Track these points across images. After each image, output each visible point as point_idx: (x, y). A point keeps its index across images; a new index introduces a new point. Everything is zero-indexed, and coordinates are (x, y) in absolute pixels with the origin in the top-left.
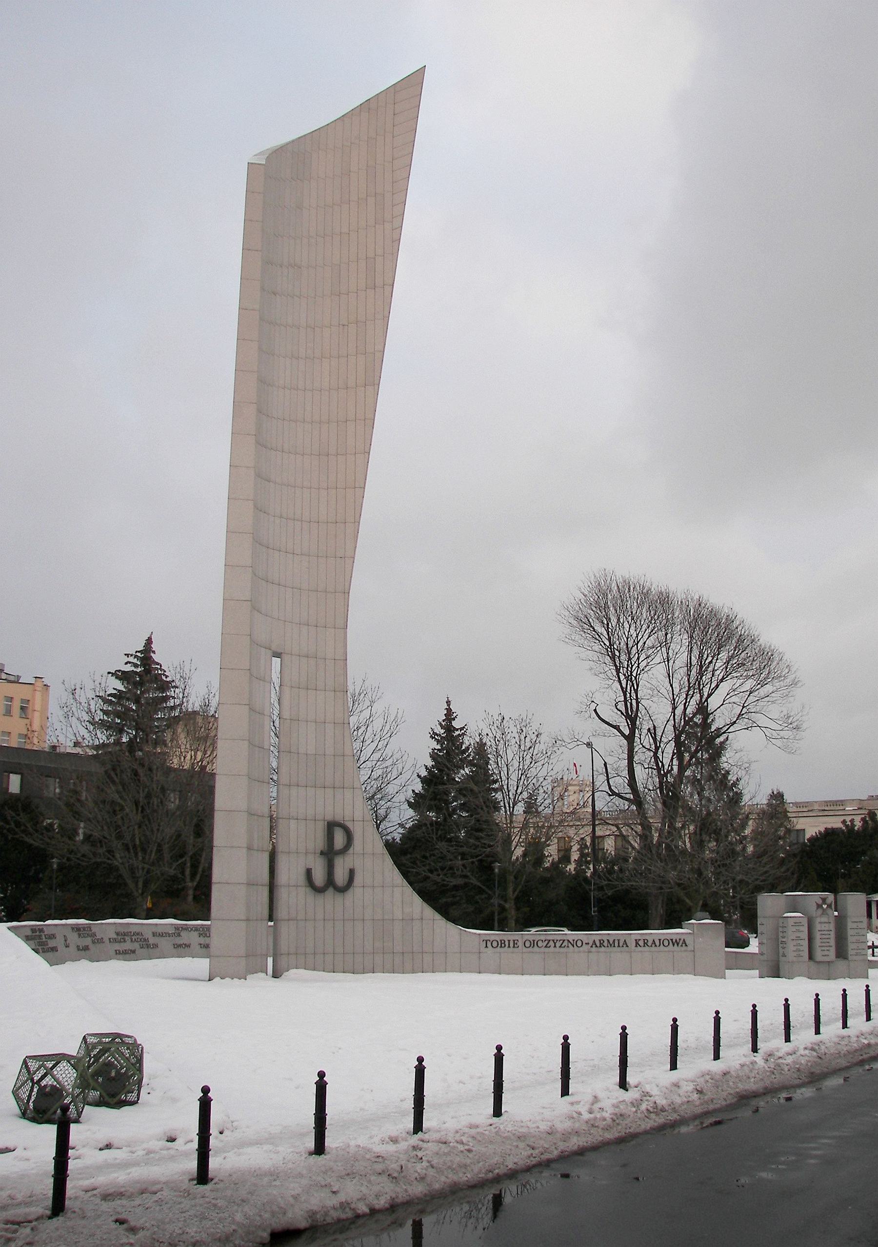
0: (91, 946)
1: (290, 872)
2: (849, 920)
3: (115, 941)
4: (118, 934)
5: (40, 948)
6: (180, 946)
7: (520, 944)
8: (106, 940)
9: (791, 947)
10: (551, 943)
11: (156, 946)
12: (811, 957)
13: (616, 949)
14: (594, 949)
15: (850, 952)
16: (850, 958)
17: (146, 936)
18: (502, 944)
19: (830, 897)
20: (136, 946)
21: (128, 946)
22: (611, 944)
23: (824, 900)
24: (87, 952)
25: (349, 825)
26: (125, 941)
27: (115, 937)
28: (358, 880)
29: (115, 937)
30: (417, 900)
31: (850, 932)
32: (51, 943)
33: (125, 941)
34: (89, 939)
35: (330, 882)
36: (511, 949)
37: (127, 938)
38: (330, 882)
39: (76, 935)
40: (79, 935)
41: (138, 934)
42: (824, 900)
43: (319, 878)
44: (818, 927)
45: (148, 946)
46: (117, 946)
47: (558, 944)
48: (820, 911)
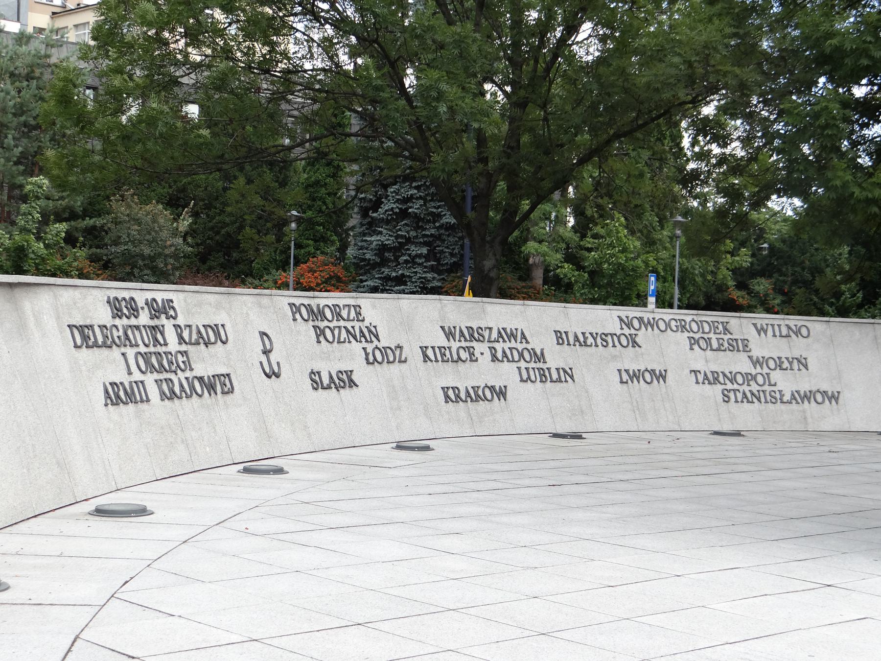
0: (362, 372)
3: (443, 355)
4: (449, 334)
5: (150, 380)
6: (635, 376)
11: (567, 374)
17: (536, 344)
20: (506, 374)
21: (483, 372)
24: (345, 393)
26: (473, 359)
27: (442, 341)
29: (442, 341)
32: (206, 362)
33: (473, 359)
34: (356, 347)
39: (306, 330)
40: (320, 333)
41: (512, 336)
45: (544, 376)
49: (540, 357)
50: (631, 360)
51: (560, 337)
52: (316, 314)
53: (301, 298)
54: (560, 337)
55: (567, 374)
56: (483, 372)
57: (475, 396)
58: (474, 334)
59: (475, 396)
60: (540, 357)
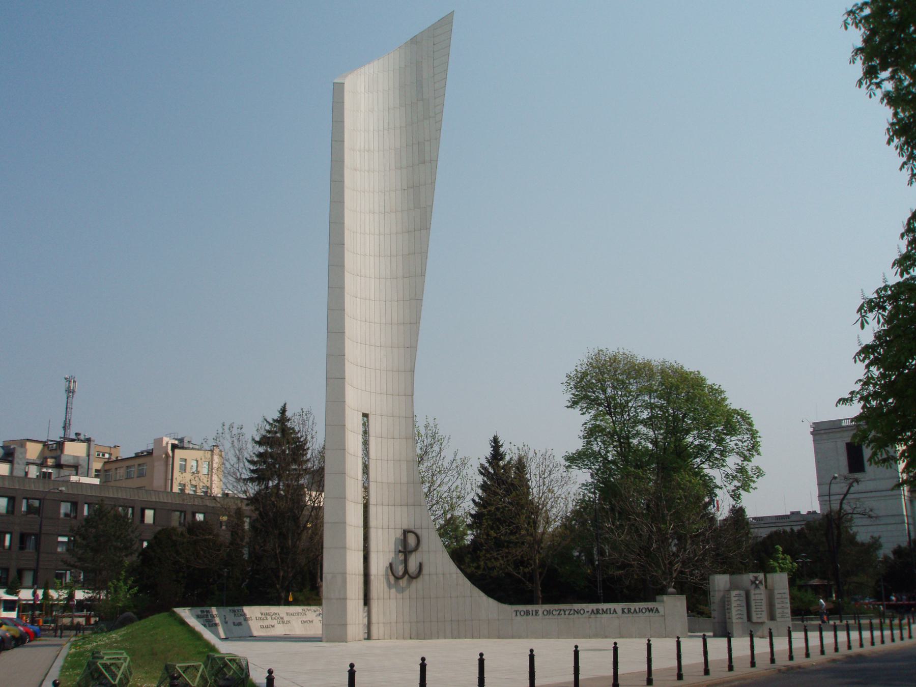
1: (378, 566)
2: (776, 592)
6: (305, 622)
7: (540, 613)
8: (254, 618)
9: (734, 612)
10: (562, 612)
11: (289, 622)
12: (749, 618)
13: (608, 616)
14: (593, 616)
15: (778, 615)
16: (778, 620)
18: (527, 613)
19: (761, 576)
20: (275, 622)
21: (269, 622)
22: (605, 612)
23: (756, 578)
25: (418, 532)
28: (425, 570)
30: (468, 583)
31: (777, 601)
35: (406, 572)
36: (534, 617)
37: (269, 617)
38: (406, 572)
42: (756, 578)
43: (400, 570)
44: (753, 597)
46: (262, 623)
47: (567, 613)
48: (754, 586)
49: (282, 618)
50: (305, 618)
51: (287, 614)
52: (234, 611)
53: (231, 608)
54: (287, 614)
55: (289, 622)
56: (269, 622)
57: (267, 627)
58: (267, 614)
59: (267, 627)
60: (282, 618)
